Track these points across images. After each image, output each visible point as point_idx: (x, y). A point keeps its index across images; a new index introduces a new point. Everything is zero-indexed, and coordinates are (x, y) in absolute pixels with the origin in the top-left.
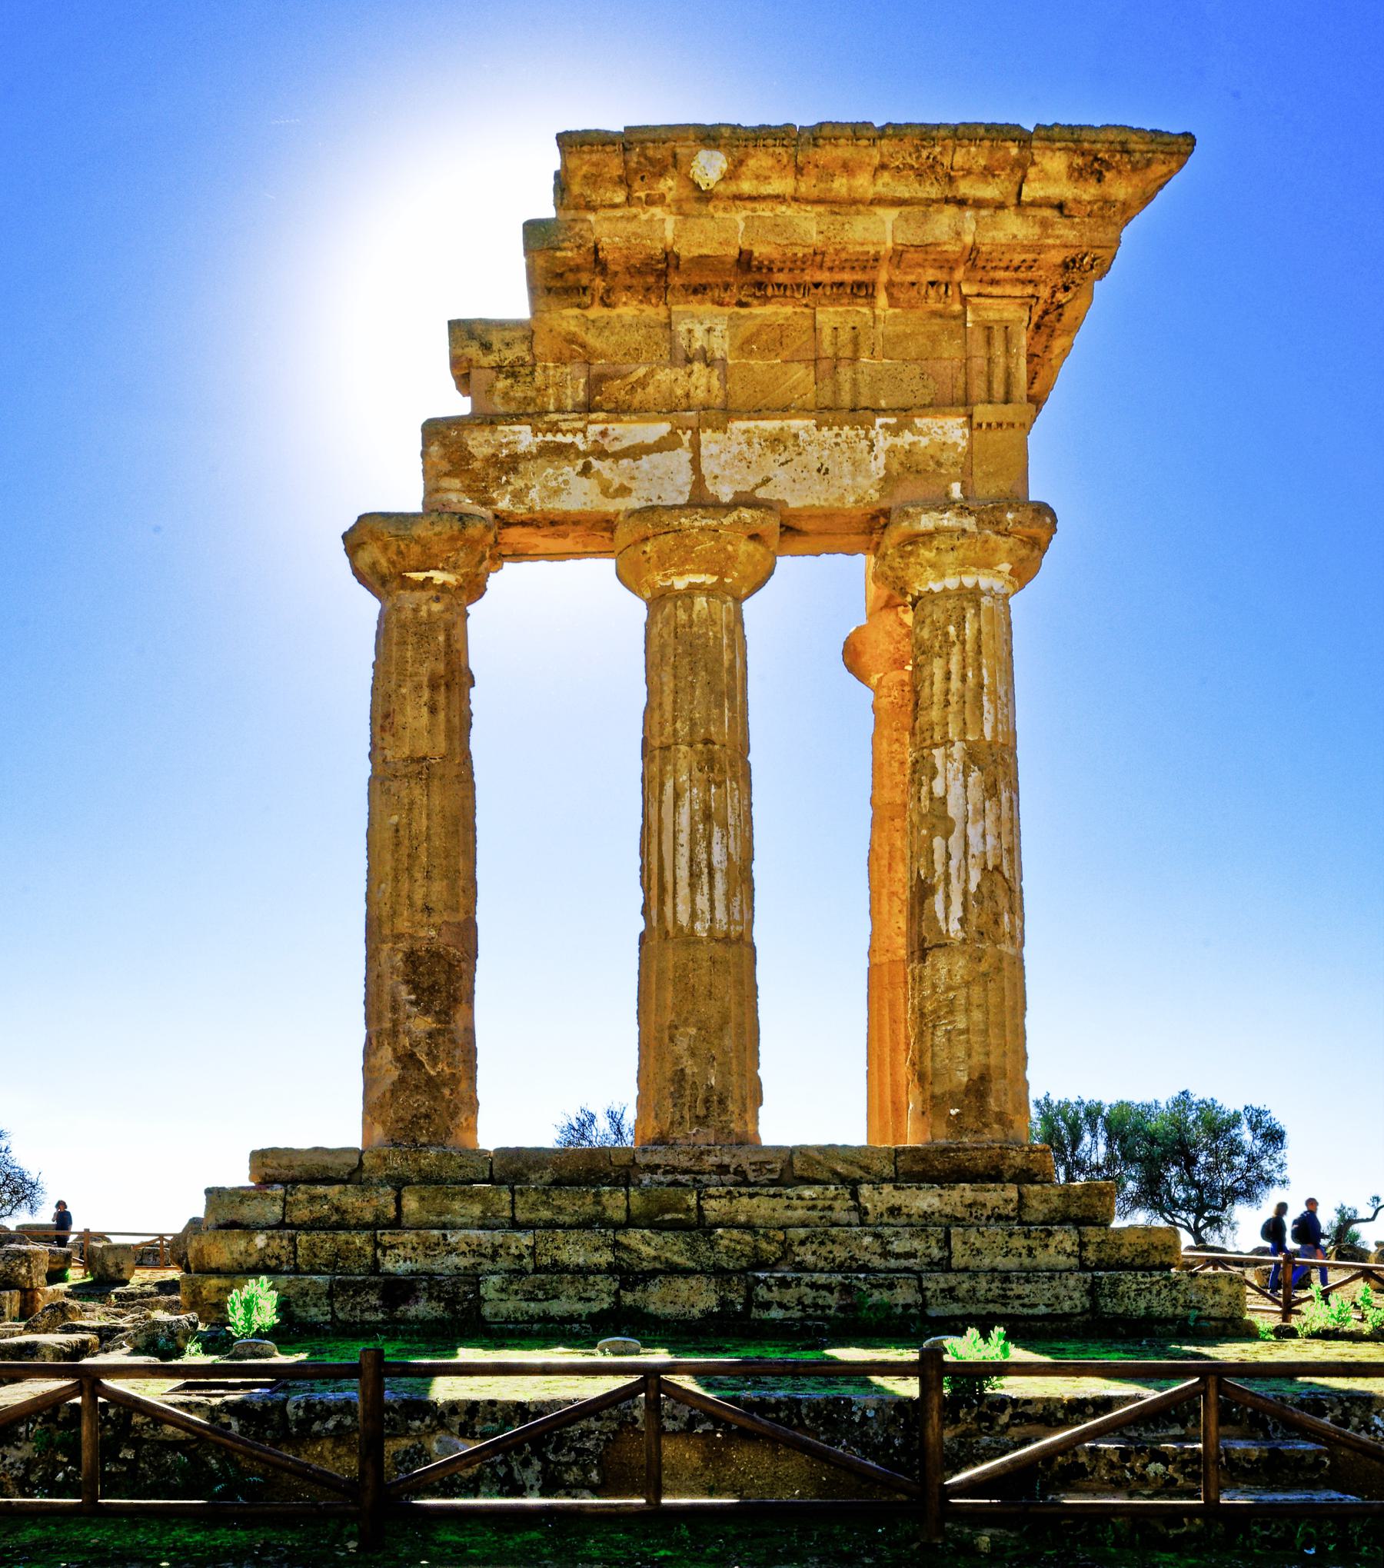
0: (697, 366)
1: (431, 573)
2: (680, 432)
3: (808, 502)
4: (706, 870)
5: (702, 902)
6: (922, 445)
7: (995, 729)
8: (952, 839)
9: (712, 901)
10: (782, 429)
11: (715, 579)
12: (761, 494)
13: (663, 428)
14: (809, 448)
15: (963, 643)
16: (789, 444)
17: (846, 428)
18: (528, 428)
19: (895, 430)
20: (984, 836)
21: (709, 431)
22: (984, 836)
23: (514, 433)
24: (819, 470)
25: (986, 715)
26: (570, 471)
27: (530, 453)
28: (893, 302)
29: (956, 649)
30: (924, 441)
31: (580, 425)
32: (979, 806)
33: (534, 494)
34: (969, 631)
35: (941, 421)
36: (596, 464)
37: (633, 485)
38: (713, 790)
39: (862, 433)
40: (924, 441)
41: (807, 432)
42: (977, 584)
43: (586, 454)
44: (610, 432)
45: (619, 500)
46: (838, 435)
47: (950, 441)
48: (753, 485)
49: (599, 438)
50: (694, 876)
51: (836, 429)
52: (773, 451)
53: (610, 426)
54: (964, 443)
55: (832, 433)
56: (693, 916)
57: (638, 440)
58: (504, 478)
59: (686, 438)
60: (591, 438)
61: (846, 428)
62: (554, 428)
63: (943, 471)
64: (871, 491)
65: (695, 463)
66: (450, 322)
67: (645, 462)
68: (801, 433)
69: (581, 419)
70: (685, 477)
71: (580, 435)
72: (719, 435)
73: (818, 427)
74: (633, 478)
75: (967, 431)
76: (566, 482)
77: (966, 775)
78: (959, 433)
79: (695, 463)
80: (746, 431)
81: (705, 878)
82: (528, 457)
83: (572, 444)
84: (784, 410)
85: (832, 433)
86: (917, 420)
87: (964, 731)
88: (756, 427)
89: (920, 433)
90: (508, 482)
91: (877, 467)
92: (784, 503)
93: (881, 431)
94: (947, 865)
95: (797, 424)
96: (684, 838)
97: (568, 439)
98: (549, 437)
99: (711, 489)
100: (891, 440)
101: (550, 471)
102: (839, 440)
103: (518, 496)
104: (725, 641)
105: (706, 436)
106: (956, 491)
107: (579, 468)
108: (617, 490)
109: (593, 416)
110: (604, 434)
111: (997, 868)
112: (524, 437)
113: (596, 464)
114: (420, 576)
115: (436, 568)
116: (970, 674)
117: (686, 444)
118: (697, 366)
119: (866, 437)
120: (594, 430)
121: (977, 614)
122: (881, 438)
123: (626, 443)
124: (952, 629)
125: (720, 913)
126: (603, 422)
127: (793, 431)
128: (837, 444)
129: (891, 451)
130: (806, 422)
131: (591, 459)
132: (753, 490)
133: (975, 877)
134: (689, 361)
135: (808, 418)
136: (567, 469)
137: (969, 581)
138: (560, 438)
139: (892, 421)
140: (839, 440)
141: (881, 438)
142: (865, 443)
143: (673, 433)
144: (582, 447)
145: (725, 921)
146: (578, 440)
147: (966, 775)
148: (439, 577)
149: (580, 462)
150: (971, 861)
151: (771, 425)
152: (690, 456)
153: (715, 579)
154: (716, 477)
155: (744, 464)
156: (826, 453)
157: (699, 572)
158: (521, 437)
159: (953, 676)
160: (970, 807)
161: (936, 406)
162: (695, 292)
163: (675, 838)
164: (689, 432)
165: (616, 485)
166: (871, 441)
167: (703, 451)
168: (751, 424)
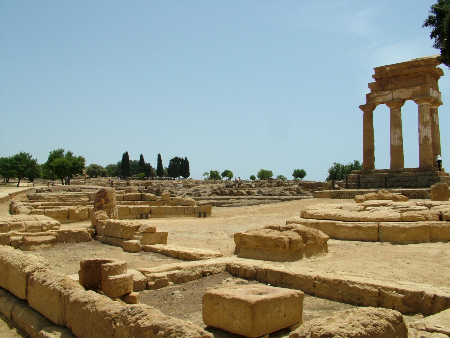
19: (413, 89)
26: (380, 97)
70: (391, 97)
82: (376, 97)
84: (400, 88)
95: (403, 89)
112: (375, 95)
125: (397, 143)
151: (400, 90)
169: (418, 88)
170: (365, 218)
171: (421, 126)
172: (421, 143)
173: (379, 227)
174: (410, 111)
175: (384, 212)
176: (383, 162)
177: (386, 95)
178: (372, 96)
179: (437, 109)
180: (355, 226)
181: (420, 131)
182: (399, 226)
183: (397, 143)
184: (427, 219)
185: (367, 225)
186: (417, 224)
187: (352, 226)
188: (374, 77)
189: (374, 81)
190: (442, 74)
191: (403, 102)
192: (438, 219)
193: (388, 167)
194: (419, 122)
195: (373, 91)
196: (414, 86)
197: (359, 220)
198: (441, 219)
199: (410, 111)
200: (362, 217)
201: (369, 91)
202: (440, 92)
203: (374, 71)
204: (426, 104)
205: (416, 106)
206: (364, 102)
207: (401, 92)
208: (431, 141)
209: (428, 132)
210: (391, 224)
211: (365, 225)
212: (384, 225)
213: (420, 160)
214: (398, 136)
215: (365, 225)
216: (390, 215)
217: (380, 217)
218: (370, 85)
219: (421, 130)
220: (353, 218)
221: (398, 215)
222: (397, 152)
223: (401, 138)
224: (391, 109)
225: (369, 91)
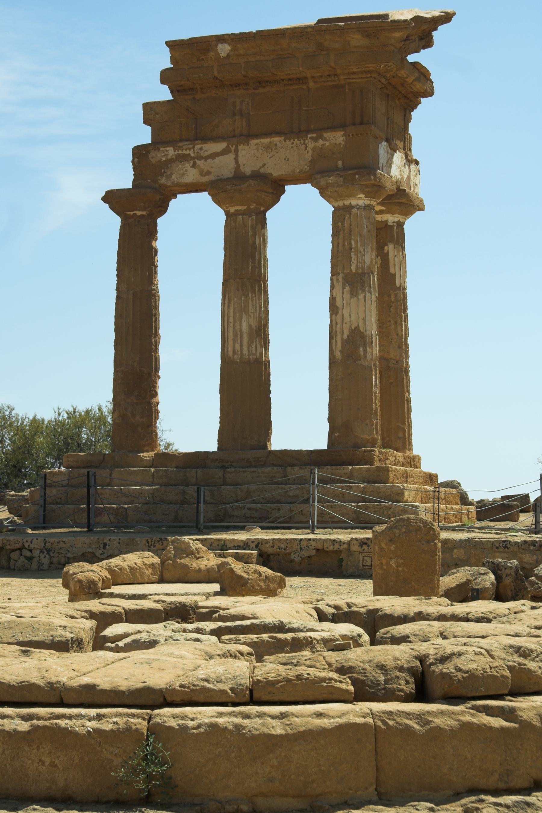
0: (237, 117)
1: (135, 212)
2: (230, 146)
3: (281, 173)
4: (239, 333)
5: (237, 347)
6: (327, 145)
7: (357, 266)
8: (338, 316)
9: (241, 345)
10: (270, 142)
11: (246, 207)
12: (262, 171)
14: (281, 150)
15: (344, 231)
16: (273, 149)
17: (296, 140)
18: (172, 148)
19: (315, 140)
20: (350, 315)
21: (242, 145)
22: (350, 315)
23: (167, 151)
24: (285, 159)
25: (353, 261)
26: (188, 166)
27: (173, 159)
28: (315, 82)
29: (341, 233)
30: (327, 143)
31: (191, 146)
32: (349, 301)
33: (174, 176)
34: (346, 224)
35: (334, 134)
36: (198, 162)
37: (212, 170)
38: (243, 299)
39: (302, 141)
40: (327, 143)
41: (280, 143)
42: (350, 203)
43: (193, 158)
44: (204, 148)
45: (206, 177)
46: (293, 143)
47: (338, 143)
48: (259, 167)
49: (199, 151)
50: (235, 336)
51: (292, 140)
52: (267, 152)
53: (203, 146)
54: (343, 143)
55: (290, 143)
56: (234, 352)
57: (214, 151)
58: (163, 170)
59: (233, 149)
60: (196, 151)
61: (296, 140)
62: (180, 148)
63: (335, 156)
64: (306, 167)
65: (236, 159)
66: (145, 106)
67: (217, 160)
68: (278, 143)
69: (191, 144)
70: (232, 165)
71: (192, 150)
72: (246, 147)
73: (285, 141)
74: (212, 167)
75: (344, 138)
76: (186, 171)
77: (343, 288)
78: (341, 139)
79: (236, 159)
80: (257, 144)
81: (239, 337)
83: (189, 155)
85: (290, 143)
86: (324, 134)
87: (343, 269)
88: (260, 142)
89: (326, 140)
90: (165, 172)
91: (308, 156)
92: (271, 174)
93: (310, 140)
94: (336, 327)
95: (276, 139)
96: (231, 319)
97: (188, 152)
98: (180, 152)
99: (242, 170)
100: (314, 144)
101: (180, 166)
102: (293, 145)
103: (169, 177)
104: (250, 233)
105: (240, 148)
106: (340, 163)
107: (191, 164)
108: (206, 173)
109: (196, 142)
110: (201, 149)
111: (357, 328)
112: (171, 152)
113: (198, 162)
114: (132, 213)
115: (136, 210)
116: (346, 244)
117: (233, 151)
118: (237, 117)
119: (304, 143)
120: (197, 147)
121: (350, 217)
122: (310, 143)
123: (210, 152)
124: (340, 224)
126: (200, 144)
127: (275, 143)
128: (292, 147)
129: (314, 149)
130: (280, 138)
131: (196, 160)
132: (259, 169)
133: (346, 333)
134: (234, 114)
135: (280, 137)
136: (187, 165)
137: (347, 203)
138: (185, 152)
139: (314, 135)
140: (293, 145)
141: (310, 143)
142: (303, 146)
143: (228, 147)
144: (192, 155)
145: (247, 354)
146: (191, 152)
147: (343, 288)
148: (139, 213)
149: (192, 162)
150: (344, 325)
151: (266, 141)
152: (234, 156)
153: (246, 207)
154: (244, 165)
155: (255, 158)
156: (288, 151)
157: (238, 205)
158: (170, 152)
159: (340, 245)
160: (344, 302)
161: (333, 128)
162: (236, 86)
163: (228, 320)
164: (234, 146)
165: (205, 171)
166: (306, 145)
167: (240, 154)
169: (337, 138)
170: (90, 688)
171: (338, 286)
172: (338, 354)
173: (156, 730)
174: (301, 227)
175: (177, 658)
176: (188, 419)
177: (214, 156)
178: (157, 156)
179: (400, 225)
180: (35, 729)
181: (334, 308)
182: (238, 727)
183: (245, 351)
184: (364, 691)
185: (91, 725)
186: (320, 715)
187: (24, 726)
188: (166, 77)
189: (164, 94)
190: (430, 93)
191: (275, 189)
192: (410, 688)
193: (209, 443)
194: (334, 273)
195: (158, 140)
196: (320, 130)
197: (59, 696)
198: (421, 694)
199: (301, 227)
200: (75, 683)
201: (144, 135)
202: (417, 163)
203: (166, 53)
204: (361, 203)
205: (325, 210)
206: (125, 180)
207: (268, 148)
208: (375, 350)
209: (366, 312)
210: (206, 714)
211: (83, 720)
212: (173, 723)
213: (330, 420)
214: (253, 323)
215: (83, 720)
216: (201, 674)
217: (159, 679)
218: (151, 112)
219: (339, 303)
220: (31, 687)
221: (240, 671)
222: (245, 386)
223: (261, 334)
224: (227, 214)
225: (144, 135)
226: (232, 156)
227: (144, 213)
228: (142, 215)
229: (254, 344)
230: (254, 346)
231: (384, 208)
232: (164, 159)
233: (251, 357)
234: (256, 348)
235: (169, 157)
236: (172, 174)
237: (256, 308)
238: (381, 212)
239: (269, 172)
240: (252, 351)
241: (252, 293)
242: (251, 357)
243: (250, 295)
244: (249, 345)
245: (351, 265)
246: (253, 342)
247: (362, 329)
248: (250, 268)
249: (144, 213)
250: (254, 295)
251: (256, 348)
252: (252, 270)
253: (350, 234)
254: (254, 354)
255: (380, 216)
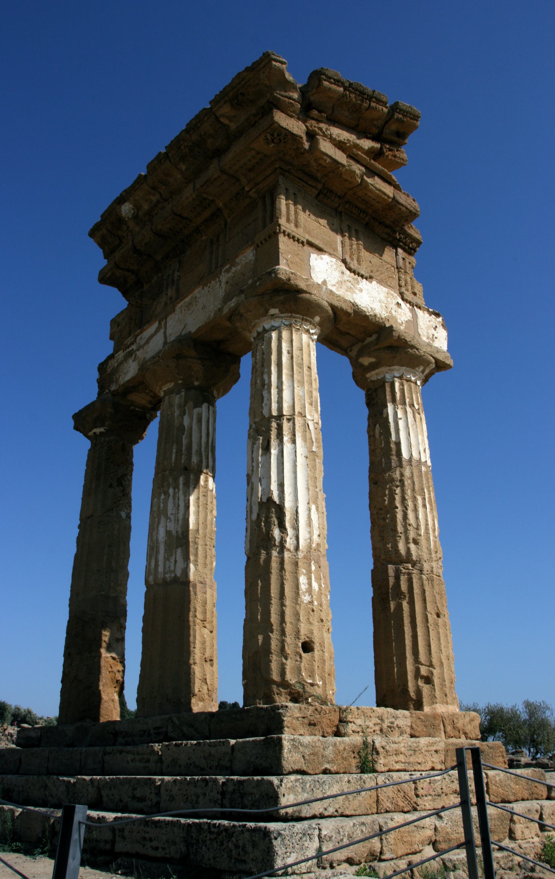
11: (173, 384)
13: (156, 325)
19: (228, 271)
30: (239, 267)
35: (245, 255)
38: (163, 497)
51: (209, 285)
68: (198, 295)
73: (203, 288)
78: (251, 254)
79: (165, 333)
80: (181, 307)
85: (207, 288)
95: (197, 291)
110: (141, 339)
112: (121, 355)
116: (258, 382)
117: (163, 326)
143: (160, 323)
153: (173, 384)
167: (168, 326)
168: (182, 303)
183: (161, 569)
226: (162, 331)
227: (102, 430)
228: (101, 433)
229: (174, 557)
230: (173, 560)
231: (373, 360)
232: (116, 365)
233: (168, 576)
234: (176, 561)
235: (120, 360)
236: (120, 376)
237: (179, 506)
238: (373, 367)
239: (189, 330)
240: (170, 567)
241: (174, 489)
242: (168, 576)
243: (171, 491)
244: (167, 559)
245: (262, 408)
246: (172, 555)
247: (276, 497)
248: (174, 456)
249: (102, 430)
250: (177, 490)
251: (176, 561)
252: (176, 459)
253: (263, 366)
254: (171, 572)
255: (373, 373)
